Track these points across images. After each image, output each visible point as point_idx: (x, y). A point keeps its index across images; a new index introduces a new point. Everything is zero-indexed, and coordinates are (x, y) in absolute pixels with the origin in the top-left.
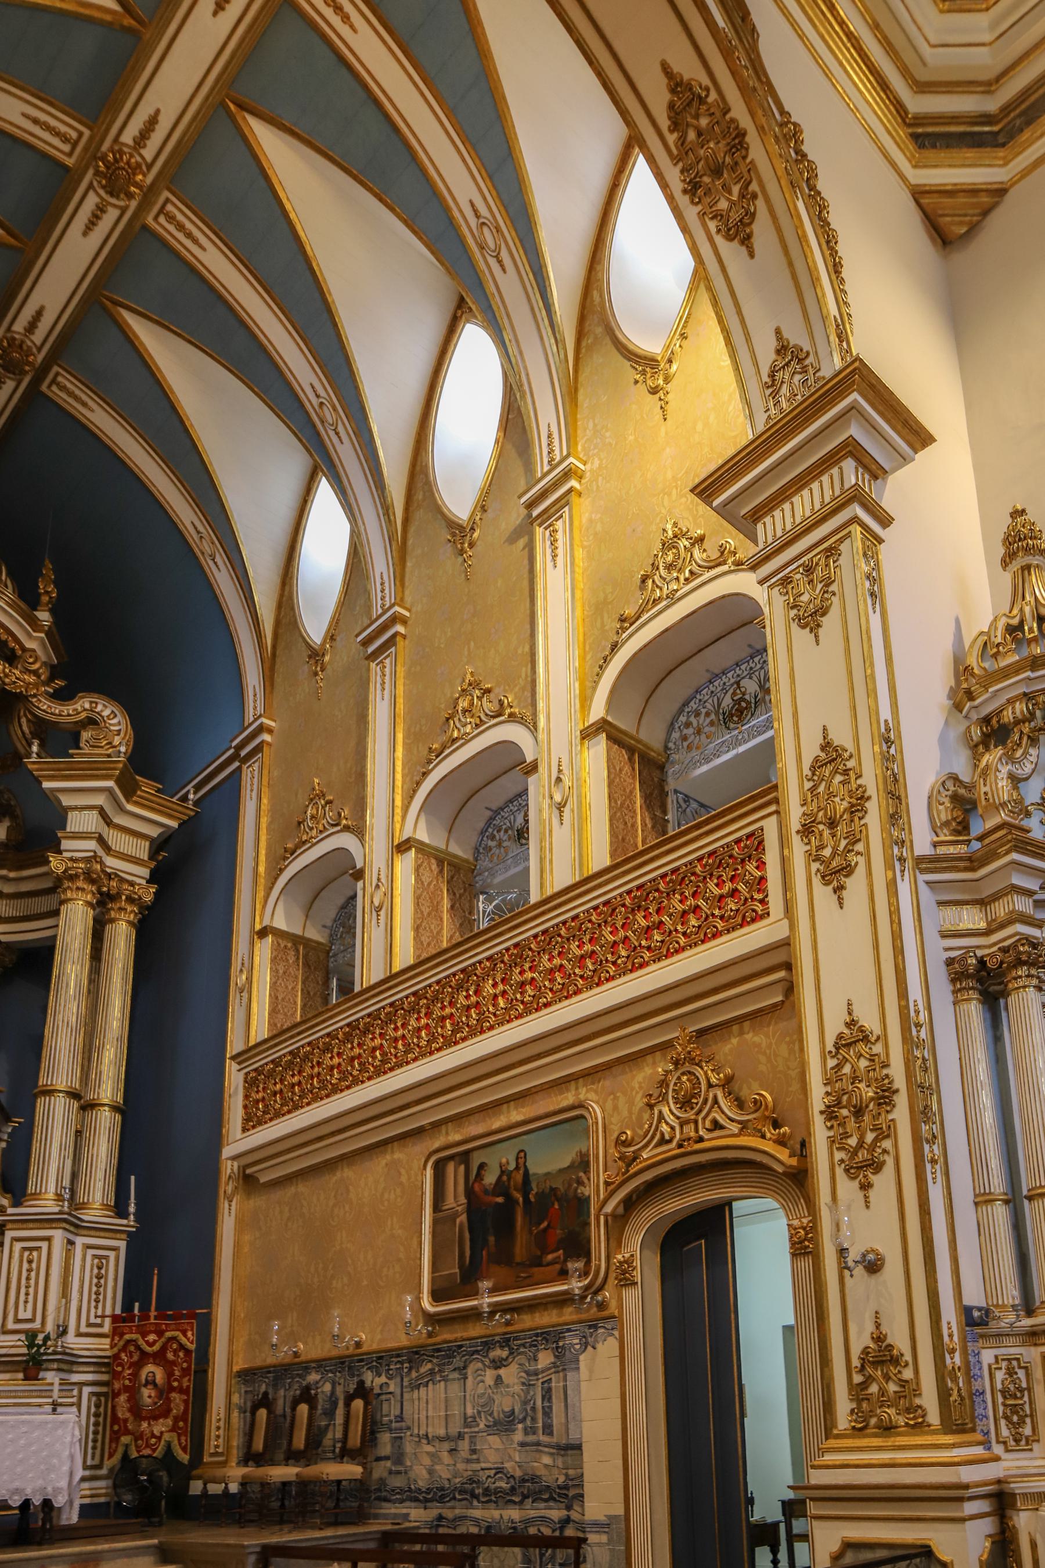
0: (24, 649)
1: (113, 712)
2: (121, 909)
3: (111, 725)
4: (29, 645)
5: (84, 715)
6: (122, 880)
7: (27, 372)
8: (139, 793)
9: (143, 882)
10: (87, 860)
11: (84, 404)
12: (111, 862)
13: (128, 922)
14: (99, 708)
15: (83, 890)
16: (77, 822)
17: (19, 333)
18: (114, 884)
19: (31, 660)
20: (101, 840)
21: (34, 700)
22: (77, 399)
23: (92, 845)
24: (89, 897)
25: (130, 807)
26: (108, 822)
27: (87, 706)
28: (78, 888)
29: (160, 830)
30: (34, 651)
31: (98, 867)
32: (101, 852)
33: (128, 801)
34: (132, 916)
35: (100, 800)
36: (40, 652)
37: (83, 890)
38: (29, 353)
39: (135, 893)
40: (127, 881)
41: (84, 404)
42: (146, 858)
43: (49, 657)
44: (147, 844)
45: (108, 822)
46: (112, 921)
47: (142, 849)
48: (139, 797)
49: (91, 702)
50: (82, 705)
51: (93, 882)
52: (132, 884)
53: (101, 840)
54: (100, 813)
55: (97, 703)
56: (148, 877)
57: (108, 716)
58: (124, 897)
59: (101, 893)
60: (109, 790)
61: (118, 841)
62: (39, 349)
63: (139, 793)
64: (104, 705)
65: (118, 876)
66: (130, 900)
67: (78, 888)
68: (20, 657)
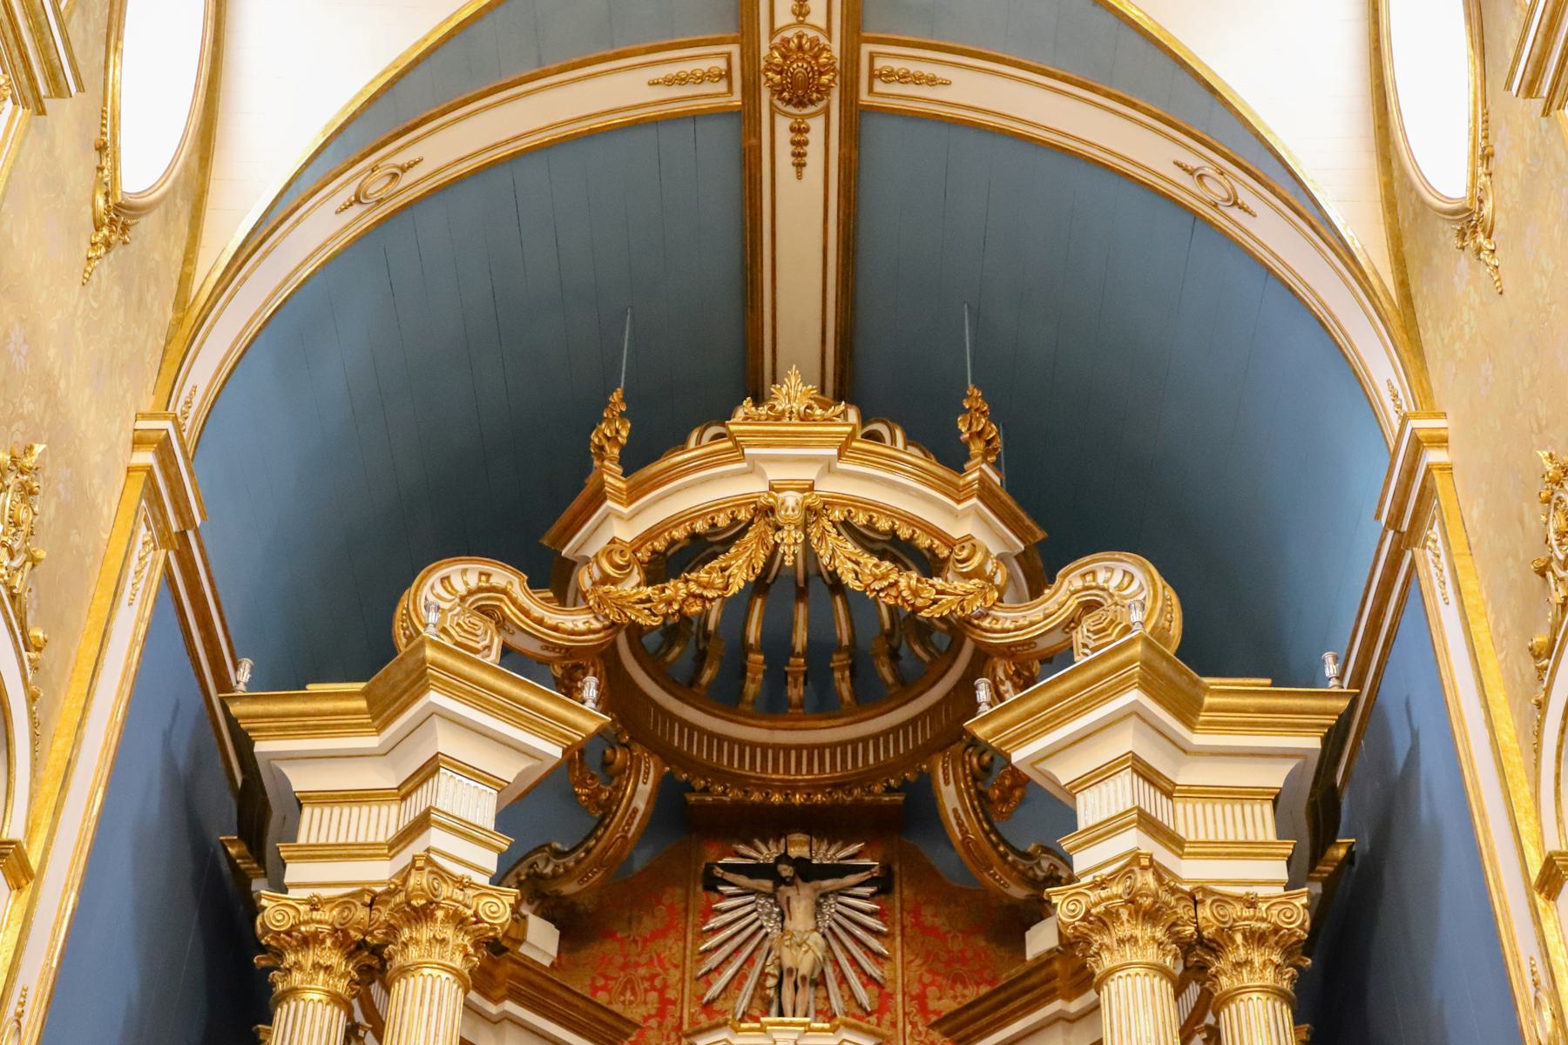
0: (950, 543)
1: (1125, 572)
2: (1238, 965)
3: (1125, 598)
4: (957, 533)
5: (1073, 603)
6: (1222, 900)
7: (829, 87)
8: (1208, 700)
9: (1280, 890)
10: (1125, 872)
11: (932, 81)
12: (1190, 871)
13: (1264, 989)
14: (1101, 577)
15: (1133, 940)
16: (1091, 808)
17: (788, 27)
18: (1205, 912)
19: (964, 554)
20: (1148, 823)
21: (986, 623)
22: (918, 79)
23: (1132, 839)
24: (1152, 954)
25: (1199, 739)
26: (1168, 790)
27: (1078, 584)
28: (1121, 941)
29: (1286, 768)
30: (969, 538)
31: (1150, 878)
32: (1148, 845)
33: (1191, 726)
34: (1269, 973)
35: (1125, 741)
36: (982, 537)
37: (1133, 940)
38: (818, 50)
39: (1263, 920)
40: (1238, 899)
41: (932, 81)
42: (1272, 837)
43: (1004, 540)
44: (1268, 807)
45: (1168, 790)
46: (1228, 998)
47: (1261, 823)
48: (1211, 709)
49: (1083, 576)
50: (1069, 585)
51: (1151, 916)
52: (1251, 903)
53: (1148, 823)
54: (1135, 771)
55: (1093, 573)
56: (1284, 876)
57: (1119, 588)
58: (1239, 938)
59: (1178, 940)
60: (1134, 712)
61: (1187, 819)
62: (828, 32)
63: (1208, 700)
64: (1108, 569)
65: (1213, 893)
66: (1257, 938)
67: (1121, 941)
68: (946, 560)
